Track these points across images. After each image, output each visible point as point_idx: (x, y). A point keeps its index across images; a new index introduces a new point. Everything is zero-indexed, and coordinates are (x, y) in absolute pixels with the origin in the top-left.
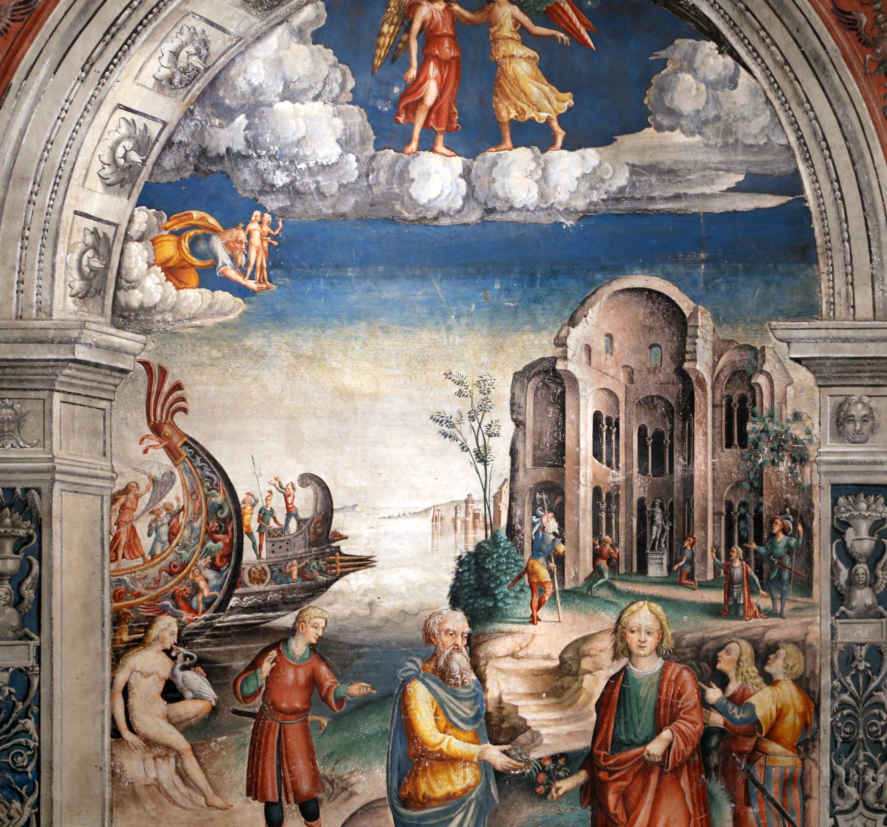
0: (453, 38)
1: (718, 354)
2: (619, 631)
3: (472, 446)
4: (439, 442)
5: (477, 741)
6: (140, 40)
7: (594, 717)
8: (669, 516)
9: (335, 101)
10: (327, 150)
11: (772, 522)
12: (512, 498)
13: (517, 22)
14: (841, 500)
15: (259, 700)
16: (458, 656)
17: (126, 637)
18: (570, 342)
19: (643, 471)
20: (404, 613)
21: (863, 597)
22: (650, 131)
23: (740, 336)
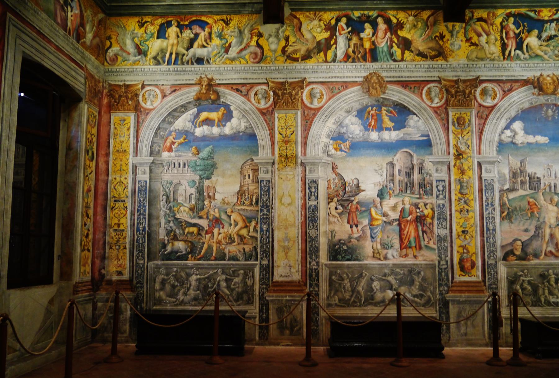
1: (417, 160)
2: (403, 201)
8: (410, 184)
10: (358, 132)
20: (370, 198)
21: (441, 196)
22: (406, 129)
23: (421, 158)
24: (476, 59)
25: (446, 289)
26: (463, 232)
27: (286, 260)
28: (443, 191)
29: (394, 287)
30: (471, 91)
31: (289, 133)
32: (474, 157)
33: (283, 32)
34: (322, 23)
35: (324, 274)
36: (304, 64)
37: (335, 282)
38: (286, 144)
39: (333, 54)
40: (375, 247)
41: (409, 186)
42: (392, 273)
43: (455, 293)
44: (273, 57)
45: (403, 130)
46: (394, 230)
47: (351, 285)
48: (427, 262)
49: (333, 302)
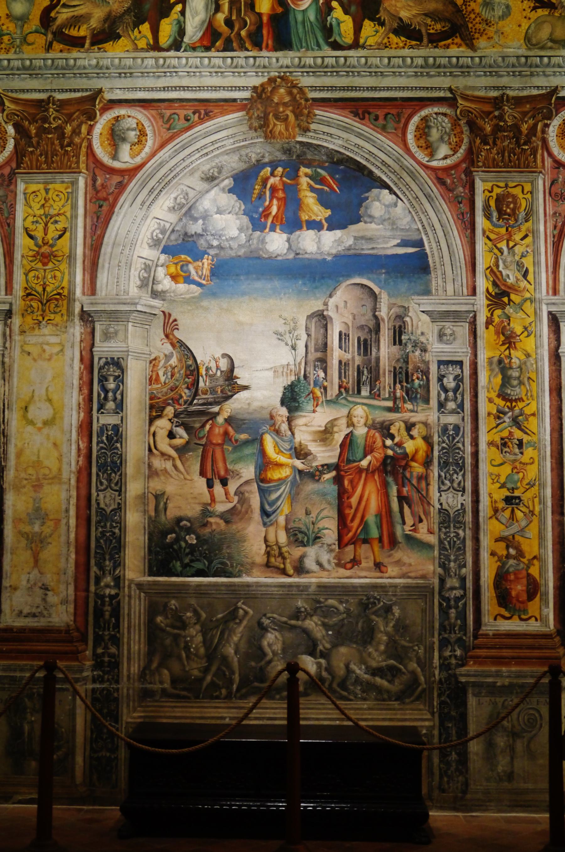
0: (283, 190)
1: (390, 309)
2: (349, 416)
3: (290, 343)
4: (277, 342)
5: (291, 457)
6: (162, 194)
7: (339, 450)
8: (370, 372)
9: (237, 214)
10: (234, 232)
11: (413, 375)
12: (306, 364)
13: (308, 184)
14: (442, 367)
15: (205, 439)
16: (283, 425)
17: (154, 414)
18: (330, 304)
19: (359, 354)
20: (262, 408)
21: (451, 405)
22: (361, 224)
23: (399, 302)
24: (550, 44)
25: (458, 653)
26: (508, 500)
27: (36, 571)
28: (456, 390)
29: (320, 647)
30: (535, 125)
31: (52, 233)
32: (540, 302)
35: (135, 609)
36: (98, 55)
37: (163, 630)
38: (45, 264)
39: (175, 28)
40: (271, 538)
41: (364, 378)
42: (315, 610)
43: (481, 664)
44: (18, 35)
45: (354, 229)
46: (324, 495)
47: (204, 642)
48: (410, 581)
49: (157, 687)
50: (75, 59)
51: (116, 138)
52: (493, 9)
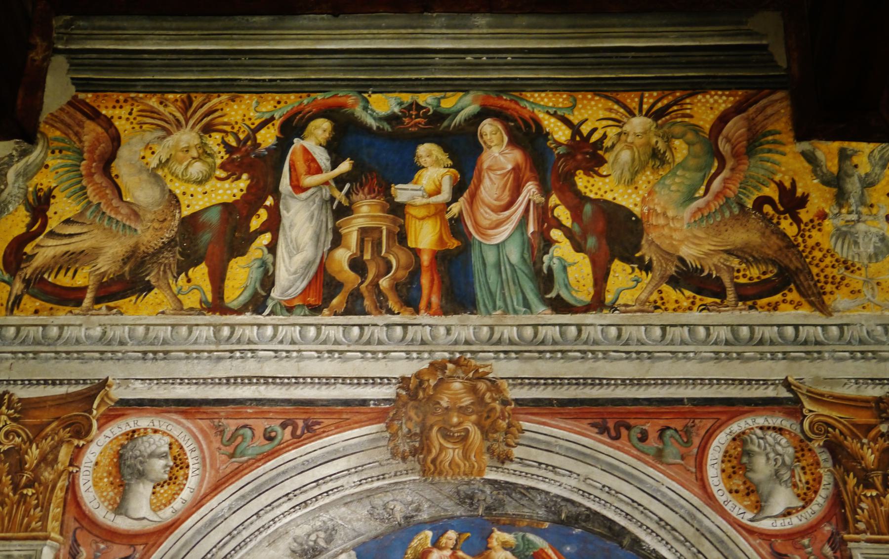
33: (26, 175)
34: (214, 141)
39: (257, 274)
50: (61, 327)
51: (126, 471)
52: (856, 243)
